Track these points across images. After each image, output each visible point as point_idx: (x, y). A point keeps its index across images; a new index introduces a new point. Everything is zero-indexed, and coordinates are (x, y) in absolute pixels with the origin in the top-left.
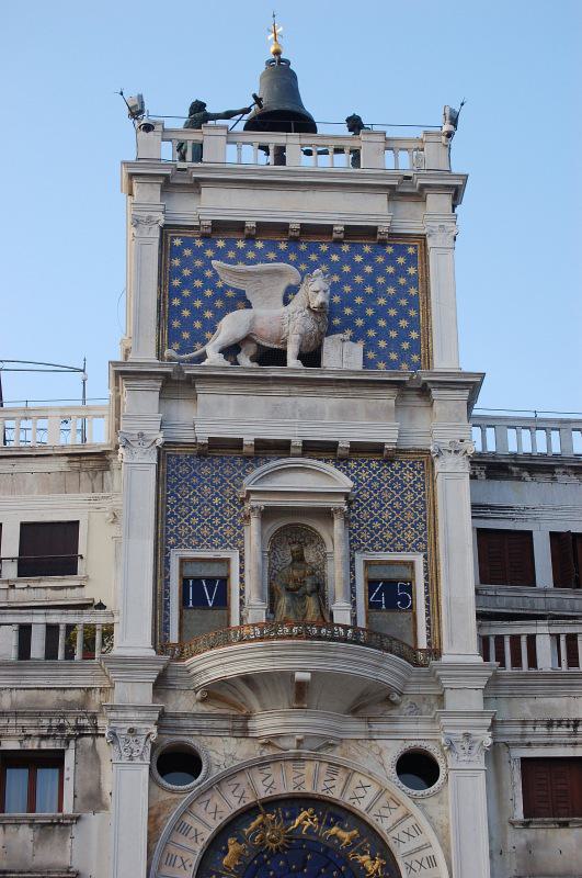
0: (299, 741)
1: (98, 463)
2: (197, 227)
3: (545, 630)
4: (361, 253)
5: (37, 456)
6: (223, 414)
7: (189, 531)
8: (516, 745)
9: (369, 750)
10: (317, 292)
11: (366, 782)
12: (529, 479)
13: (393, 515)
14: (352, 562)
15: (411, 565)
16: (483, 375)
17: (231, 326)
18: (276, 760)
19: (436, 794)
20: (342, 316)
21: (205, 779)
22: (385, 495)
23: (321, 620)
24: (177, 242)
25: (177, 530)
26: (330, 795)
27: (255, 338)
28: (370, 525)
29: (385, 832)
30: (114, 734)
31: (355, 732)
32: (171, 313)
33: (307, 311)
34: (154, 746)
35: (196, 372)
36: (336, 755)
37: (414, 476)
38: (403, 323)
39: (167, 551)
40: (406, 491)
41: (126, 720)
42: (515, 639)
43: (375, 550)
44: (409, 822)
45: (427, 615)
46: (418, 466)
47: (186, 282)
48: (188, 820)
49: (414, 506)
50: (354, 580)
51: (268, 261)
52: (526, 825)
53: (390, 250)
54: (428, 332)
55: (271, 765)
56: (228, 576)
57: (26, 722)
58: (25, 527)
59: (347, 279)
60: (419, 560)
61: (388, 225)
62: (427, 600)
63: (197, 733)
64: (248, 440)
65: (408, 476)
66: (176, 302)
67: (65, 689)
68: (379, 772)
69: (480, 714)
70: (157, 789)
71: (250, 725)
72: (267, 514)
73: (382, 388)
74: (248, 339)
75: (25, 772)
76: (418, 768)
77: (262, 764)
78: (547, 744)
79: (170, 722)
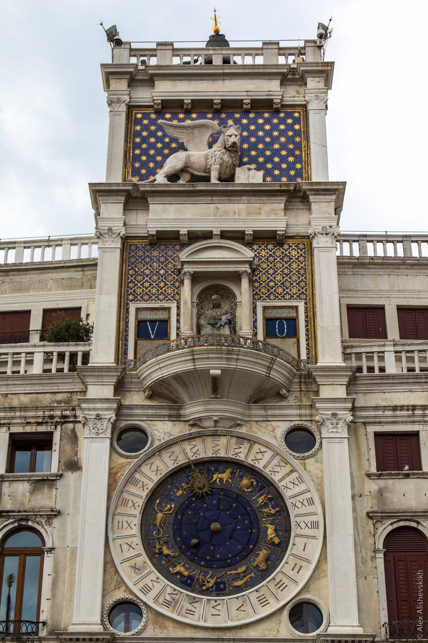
0: (216, 422)
3: (392, 348)
4: (262, 118)
7: (143, 291)
9: (266, 428)
13: (283, 278)
15: (296, 308)
17: (174, 162)
18: (200, 436)
19: (312, 456)
20: (249, 156)
22: (278, 265)
24: (139, 116)
25: (134, 291)
26: (238, 458)
27: (189, 170)
29: (277, 482)
30: (86, 419)
31: (256, 416)
33: (224, 150)
37: (298, 253)
38: (291, 159)
39: (128, 304)
40: (292, 262)
41: (95, 409)
44: (295, 475)
46: (301, 246)
47: (144, 140)
50: (256, 319)
52: (379, 476)
53: (282, 115)
54: (308, 164)
55: (197, 440)
56: (169, 318)
59: (253, 134)
61: (281, 97)
62: (307, 330)
64: (183, 231)
65: (294, 253)
66: (137, 152)
68: (273, 442)
69: (344, 400)
70: (115, 456)
71: (182, 412)
72: (196, 278)
76: (301, 440)
78: (393, 422)
79: (126, 411)
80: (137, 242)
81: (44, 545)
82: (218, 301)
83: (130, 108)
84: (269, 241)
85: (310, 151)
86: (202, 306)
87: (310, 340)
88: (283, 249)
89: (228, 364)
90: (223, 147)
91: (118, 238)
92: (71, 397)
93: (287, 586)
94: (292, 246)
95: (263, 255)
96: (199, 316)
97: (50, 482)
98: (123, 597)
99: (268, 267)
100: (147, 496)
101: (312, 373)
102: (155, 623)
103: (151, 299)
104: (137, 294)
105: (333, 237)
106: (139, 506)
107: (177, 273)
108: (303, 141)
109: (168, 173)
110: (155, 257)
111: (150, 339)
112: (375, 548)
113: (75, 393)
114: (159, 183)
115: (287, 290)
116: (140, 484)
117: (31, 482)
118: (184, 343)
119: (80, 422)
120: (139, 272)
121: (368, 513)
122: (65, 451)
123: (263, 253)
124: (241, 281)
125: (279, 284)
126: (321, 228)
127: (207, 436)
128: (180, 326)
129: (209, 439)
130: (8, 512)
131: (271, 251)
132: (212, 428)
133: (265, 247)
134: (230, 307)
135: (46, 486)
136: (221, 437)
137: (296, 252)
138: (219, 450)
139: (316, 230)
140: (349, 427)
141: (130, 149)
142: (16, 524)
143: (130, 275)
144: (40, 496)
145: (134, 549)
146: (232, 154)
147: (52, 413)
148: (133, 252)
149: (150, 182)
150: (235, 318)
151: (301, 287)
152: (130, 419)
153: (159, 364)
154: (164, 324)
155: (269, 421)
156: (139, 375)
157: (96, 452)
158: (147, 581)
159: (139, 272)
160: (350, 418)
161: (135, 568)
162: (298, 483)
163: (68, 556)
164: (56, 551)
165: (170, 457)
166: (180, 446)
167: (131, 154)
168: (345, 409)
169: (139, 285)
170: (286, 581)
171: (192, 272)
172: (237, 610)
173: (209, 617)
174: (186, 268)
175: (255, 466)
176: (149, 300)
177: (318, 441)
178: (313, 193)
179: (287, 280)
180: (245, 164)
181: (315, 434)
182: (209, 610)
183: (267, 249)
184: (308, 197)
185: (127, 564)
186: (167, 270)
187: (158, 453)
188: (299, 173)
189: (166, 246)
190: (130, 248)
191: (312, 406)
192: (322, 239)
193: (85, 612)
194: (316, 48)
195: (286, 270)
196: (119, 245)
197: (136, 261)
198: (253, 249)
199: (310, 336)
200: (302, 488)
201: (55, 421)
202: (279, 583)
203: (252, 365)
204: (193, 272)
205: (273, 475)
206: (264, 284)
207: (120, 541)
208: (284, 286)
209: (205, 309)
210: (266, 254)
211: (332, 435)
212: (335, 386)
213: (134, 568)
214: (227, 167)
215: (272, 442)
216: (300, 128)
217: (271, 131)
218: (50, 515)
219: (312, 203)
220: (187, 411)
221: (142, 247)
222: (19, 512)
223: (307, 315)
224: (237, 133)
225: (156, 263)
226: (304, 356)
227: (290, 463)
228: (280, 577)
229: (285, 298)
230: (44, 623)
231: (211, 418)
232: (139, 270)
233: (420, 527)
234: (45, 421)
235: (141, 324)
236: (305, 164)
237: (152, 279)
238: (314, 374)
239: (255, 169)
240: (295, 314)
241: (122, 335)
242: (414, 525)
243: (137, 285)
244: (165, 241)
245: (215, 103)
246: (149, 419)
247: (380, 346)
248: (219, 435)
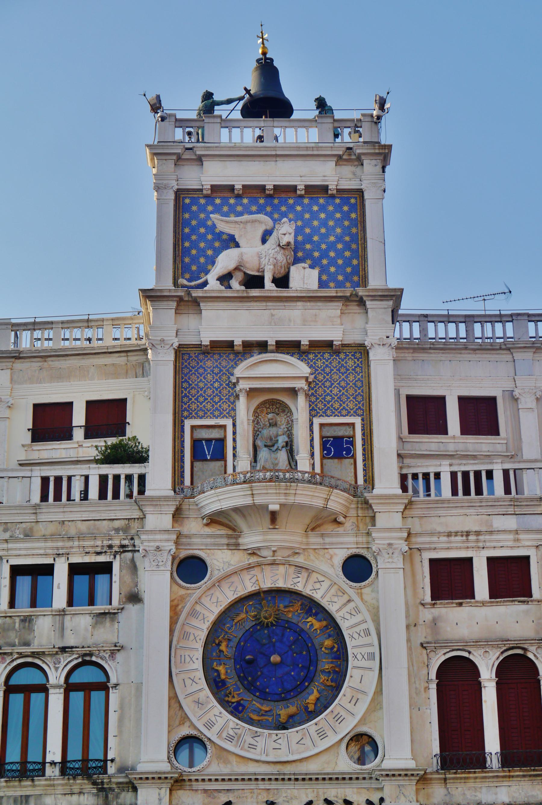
0: (274, 551)
2: (201, 190)
4: (317, 204)
6: (219, 323)
7: (198, 406)
8: (425, 549)
10: (285, 234)
11: (321, 578)
13: (340, 391)
14: (311, 425)
15: (353, 425)
16: (402, 290)
17: (226, 261)
18: (259, 565)
19: (369, 585)
20: (304, 250)
21: (209, 579)
23: (289, 467)
24: (187, 201)
25: (189, 406)
26: (296, 588)
27: (242, 268)
29: (335, 613)
32: (183, 253)
33: (278, 248)
34: (174, 558)
35: (201, 295)
37: (355, 363)
39: (183, 421)
40: (349, 374)
41: (155, 541)
43: (327, 416)
44: (352, 605)
45: (364, 461)
46: (358, 355)
48: (198, 608)
49: (355, 384)
50: (313, 438)
51: (251, 213)
53: (338, 201)
54: (365, 259)
55: (256, 569)
56: (225, 437)
58: (90, 404)
60: (357, 421)
61: (336, 183)
62: (364, 450)
64: (238, 342)
65: (350, 363)
67: (113, 519)
70: (176, 587)
71: (241, 541)
74: (237, 269)
76: (358, 568)
77: (249, 568)
79: (184, 540)
80: (190, 351)
82: (274, 420)
83: (179, 194)
88: (339, 359)
89: (286, 499)
90: (277, 244)
91: (170, 349)
92: (129, 524)
94: (348, 355)
95: (319, 366)
96: (255, 437)
97: (112, 616)
98: (188, 733)
101: (368, 501)
102: (219, 758)
104: (191, 410)
107: (232, 387)
110: (209, 368)
111: (206, 460)
112: (428, 679)
113: (133, 520)
114: (211, 289)
116: (201, 617)
117: (92, 615)
121: (422, 644)
122: (125, 582)
123: (319, 363)
125: (336, 398)
130: (72, 647)
131: (327, 361)
133: (321, 356)
135: (108, 620)
137: (353, 361)
141: (179, 241)
142: (80, 660)
143: (182, 388)
144: (102, 630)
146: (287, 252)
147: (110, 542)
148: (186, 362)
155: (327, 549)
156: (197, 503)
157: (157, 582)
159: (193, 385)
161: (199, 703)
162: (355, 614)
167: (181, 247)
168: (401, 538)
169: (193, 399)
170: (343, 713)
171: (248, 389)
173: (271, 751)
176: (204, 416)
177: (374, 570)
178: (370, 298)
179: (343, 393)
181: (372, 562)
183: (324, 359)
184: (365, 302)
185: (190, 699)
186: (222, 383)
189: (220, 355)
190: (182, 357)
191: (368, 534)
193: (152, 753)
194: (373, 124)
196: (172, 358)
199: (366, 456)
200: (358, 618)
201: (113, 551)
203: (311, 497)
204: (249, 388)
205: (331, 605)
206: (320, 398)
207: (183, 676)
208: (341, 401)
209: (261, 424)
211: (388, 566)
212: (391, 513)
213: (198, 702)
214: (281, 267)
216: (357, 216)
218: (114, 650)
221: (195, 357)
222: (83, 647)
225: (211, 374)
226: (361, 481)
228: (339, 709)
230: (112, 761)
231: (270, 548)
233: (471, 657)
237: (206, 393)
238: (370, 501)
240: (352, 433)
241: (178, 456)
242: (466, 654)
244: (218, 349)
245: (268, 189)
247: (436, 465)
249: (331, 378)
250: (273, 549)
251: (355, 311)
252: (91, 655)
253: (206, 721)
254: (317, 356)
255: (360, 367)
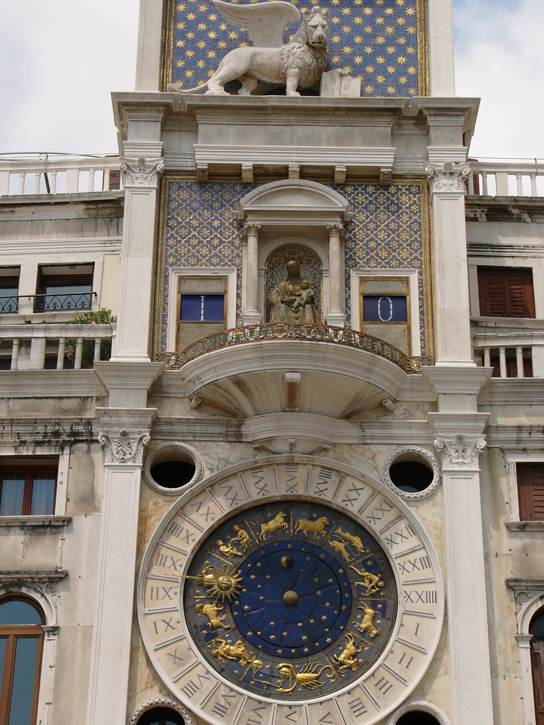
1: (113, 211)
5: (56, 204)
7: (189, 251)
11: (359, 485)
12: (528, 220)
13: (389, 235)
14: (348, 279)
17: (233, 63)
18: (270, 464)
19: (429, 497)
20: (341, 54)
21: (197, 481)
26: (323, 497)
28: (366, 245)
30: (107, 438)
31: (349, 437)
34: (147, 450)
36: (329, 460)
39: (166, 270)
40: (402, 213)
41: (119, 425)
42: (511, 352)
46: (414, 189)
49: (410, 227)
50: (349, 296)
52: (522, 528)
54: (426, 69)
55: (265, 469)
56: (226, 292)
57: (21, 428)
59: (347, 20)
62: (422, 313)
63: (191, 438)
64: (247, 165)
66: (180, 44)
67: (61, 398)
68: (373, 476)
70: (148, 492)
72: (263, 235)
73: (379, 116)
75: (21, 484)
76: (412, 474)
80: (180, 179)
81: (44, 621)
84: (368, 182)
85: (428, 48)
86: (273, 273)
87: (426, 327)
88: (388, 193)
90: (306, 41)
93: (391, 686)
94: (401, 190)
95: (360, 202)
96: (269, 289)
99: (367, 219)
100: (193, 551)
103: (200, 263)
104: (179, 255)
105: (460, 178)
106: (181, 566)
108: (418, 33)
109: (226, 79)
110: (207, 202)
112: (518, 633)
113: (90, 399)
115: (394, 254)
117: (25, 529)
118: (249, 335)
119: (97, 441)
120: (183, 224)
121: (508, 581)
123: (360, 198)
124: (329, 241)
125: (383, 244)
126: (443, 164)
127: (278, 464)
128: (241, 303)
129: (283, 468)
132: (287, 453)
134: (313, 275)
136: (299, 466)
137: (407, 197)
138: (297, 485)
139: (436, 168)
140: (480, 455)
141: (169, 39)
143: (168, 226)
145: (173, 629)
146: (318, 53)
149: (197, 92)
150: (320, 294)
151: (413, 249)
152: (169, 438)
153: (212, 362)
154: (217, 300)
155: (367, 444)
156: (183, 376)
157: (120, 485)
158: (193, 676)
159: (183, 224)
160: (483, 443)
161: (175, 657)
163: (79, 638)
164: (62, 631)
165: (225, 495)
166: (241, 479)
167: (172, 47)
169: (183, 241)
170: (388, 677)
171: (259, 227)
172: (320, 721)
174: (250, 220)
175: (347, 510)
178: (433, 112)
179: (393, 238)
180: (336, 66)
182: (280, 721)
183: (366, 193)
184: (426, 118)
187: (210, 489)
188: (413, 81)
190: (170, 187)
192: (445, 181)
195: (393, 224)
197: (178, 207)
198: (345, 193)
201: (61, 440)
202: (381, 681)
204: (261, 226)
205: (373, 523)
206: (361, 244)
207: (153, 618)
208: (390, 248)
209: (277, 279)
210: (364, 200)
214: (309, 71)
215: (371, 476)
217: (373, 17)
219: (431, 127)
220: (251, 429)
223: (422, 290)
224: (325, 23)
227: (396, 507)
228: (382, 672)
229: (391, 265)
232: (183, 220)
234: (47, 440)
235: (188, 300)
236: (421, 68)
239: (349, 74)
243: (180, 241)
244: (220, 178)
246: (196, 439)
248: (297, 464)
249: (376, 218)
250: (292, 441)
251: (411, 132)
252: (20, 583)
253: (185, 684)
254: (357, 189)
255: (417, 205)
